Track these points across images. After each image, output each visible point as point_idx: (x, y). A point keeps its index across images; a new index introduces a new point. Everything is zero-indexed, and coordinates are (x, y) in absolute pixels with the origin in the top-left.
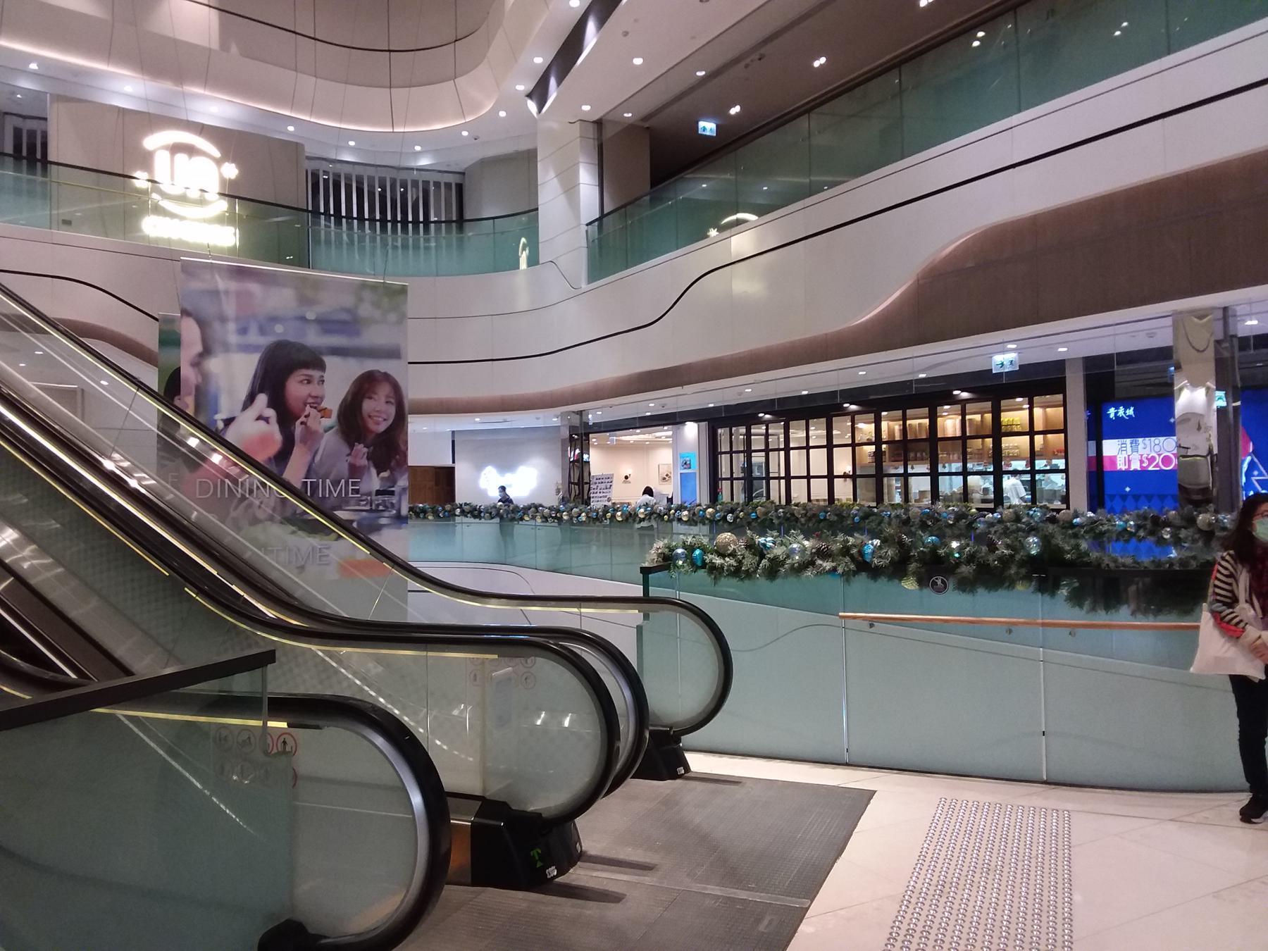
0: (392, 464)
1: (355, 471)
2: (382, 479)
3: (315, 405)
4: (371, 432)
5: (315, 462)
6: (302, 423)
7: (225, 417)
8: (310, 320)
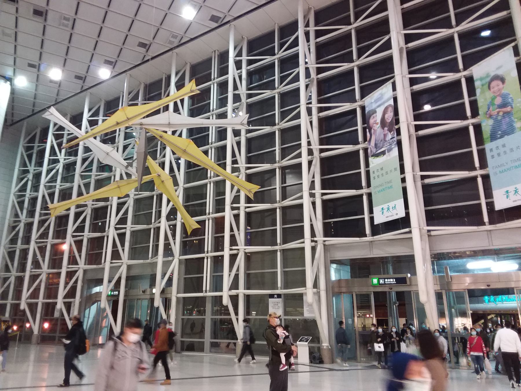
1: (385, 135)
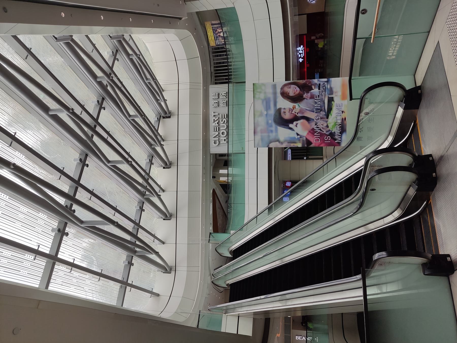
0: (310, 85)
1: (312, 97)
2: (315, 88)
3: (292, 110)
4: (299, 93)
5: (309, 109)
6: (297, 114)
7: (296, 135)
8: (267, 113)
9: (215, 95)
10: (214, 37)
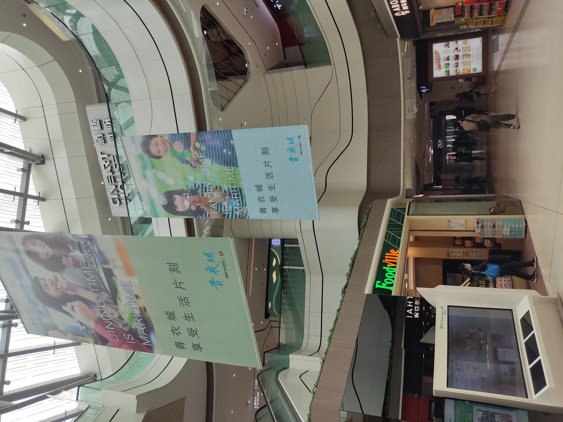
1: (76, 264)
6: (67, 291)
7: (79, 325)
9: (95, 124)
10: (58, 27)
